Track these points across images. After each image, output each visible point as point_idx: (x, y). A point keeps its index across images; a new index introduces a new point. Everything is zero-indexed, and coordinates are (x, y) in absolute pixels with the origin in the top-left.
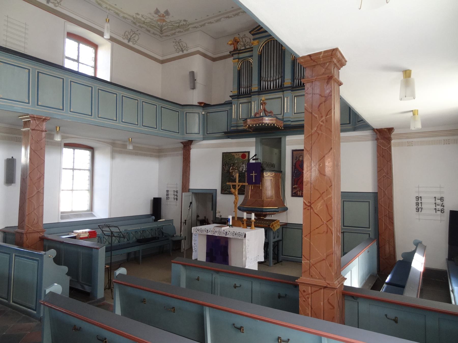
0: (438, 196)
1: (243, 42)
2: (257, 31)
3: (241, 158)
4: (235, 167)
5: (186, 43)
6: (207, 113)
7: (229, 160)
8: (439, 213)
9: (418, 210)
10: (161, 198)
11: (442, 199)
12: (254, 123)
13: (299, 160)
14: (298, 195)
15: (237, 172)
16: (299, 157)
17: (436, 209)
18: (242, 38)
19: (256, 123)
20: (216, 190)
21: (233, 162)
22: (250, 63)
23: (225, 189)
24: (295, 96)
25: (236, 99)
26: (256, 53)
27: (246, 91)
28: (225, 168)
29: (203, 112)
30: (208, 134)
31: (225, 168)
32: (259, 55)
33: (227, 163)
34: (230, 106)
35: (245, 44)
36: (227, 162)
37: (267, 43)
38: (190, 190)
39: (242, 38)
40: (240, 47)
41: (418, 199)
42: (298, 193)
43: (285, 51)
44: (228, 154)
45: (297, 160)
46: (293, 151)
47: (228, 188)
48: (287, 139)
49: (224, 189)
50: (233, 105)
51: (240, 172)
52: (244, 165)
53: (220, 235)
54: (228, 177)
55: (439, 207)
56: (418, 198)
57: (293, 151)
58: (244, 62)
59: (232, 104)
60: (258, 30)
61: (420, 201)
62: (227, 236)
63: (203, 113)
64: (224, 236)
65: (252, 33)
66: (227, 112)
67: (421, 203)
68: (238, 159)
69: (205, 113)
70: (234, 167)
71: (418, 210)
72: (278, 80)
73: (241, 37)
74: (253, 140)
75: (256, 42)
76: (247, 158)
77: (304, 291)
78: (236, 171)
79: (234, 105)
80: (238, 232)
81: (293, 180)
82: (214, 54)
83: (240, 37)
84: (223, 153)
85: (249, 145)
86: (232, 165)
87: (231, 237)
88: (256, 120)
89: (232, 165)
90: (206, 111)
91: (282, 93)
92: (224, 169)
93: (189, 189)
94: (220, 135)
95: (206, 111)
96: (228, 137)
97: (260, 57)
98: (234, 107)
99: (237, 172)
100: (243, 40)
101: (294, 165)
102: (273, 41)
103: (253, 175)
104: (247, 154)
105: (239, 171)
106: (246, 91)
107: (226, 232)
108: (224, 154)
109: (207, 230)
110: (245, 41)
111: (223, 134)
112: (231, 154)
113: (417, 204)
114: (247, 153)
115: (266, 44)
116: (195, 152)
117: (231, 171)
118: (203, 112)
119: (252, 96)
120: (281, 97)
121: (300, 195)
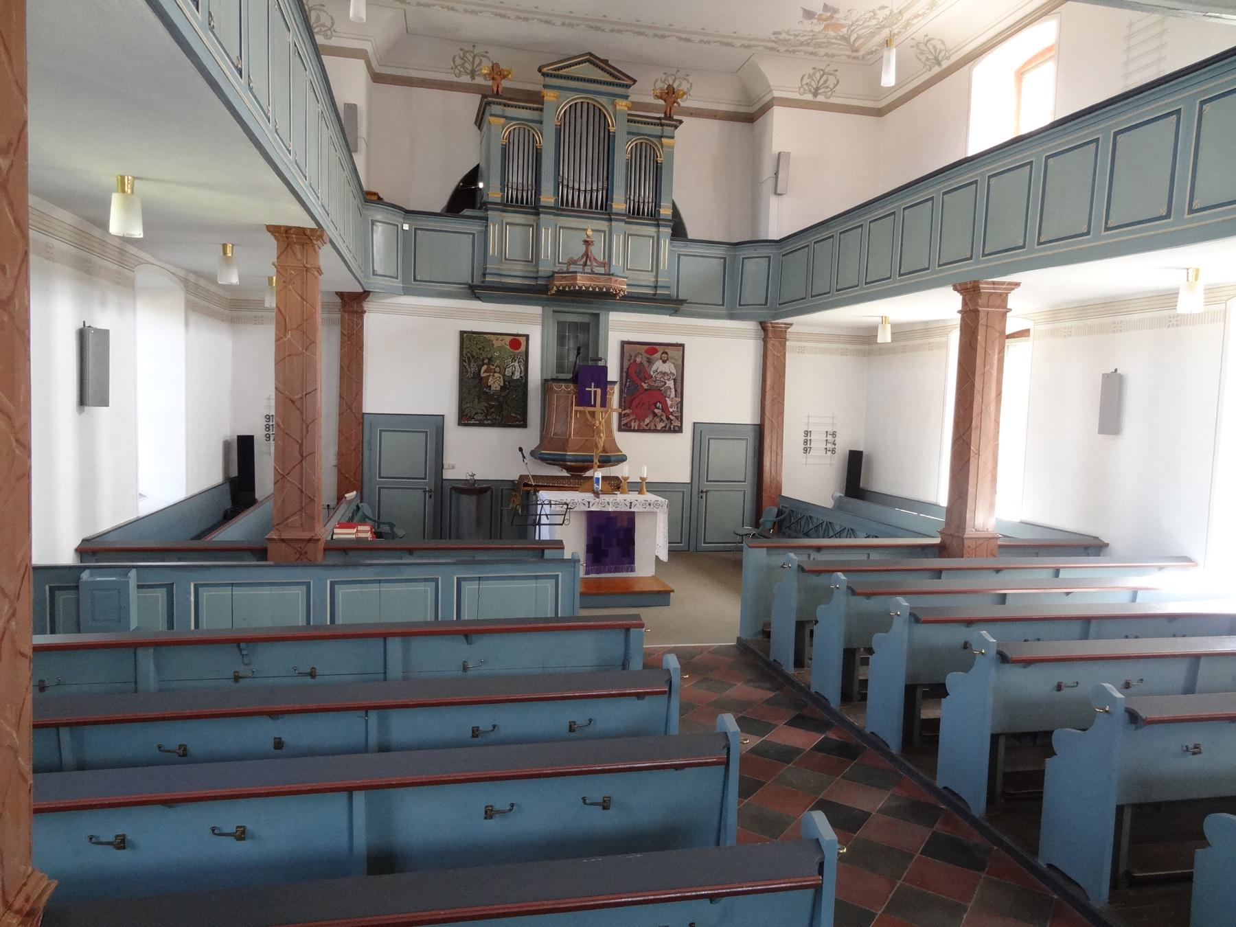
0: (830, 430)
1: (473, 64)
3: (508, 347)
4: (493, 365)
5: (332, 19)
6: (416, 229)
7: (480, 349)
8: (829, 453)
9: (806, 450)
10: (253, 436)
11: (834, 434)
13: (635, 361)
14: (632, 428)
15: (500, 377)
16: (636, 356)
17: (826, 449)
20: (443, 416)
21: (489, 356)
22: (531, 136)
23: (469, 414)
24: (629, 235)
26: (551, 120)
27: (520, 197)
28: (470, 367)
29: (404, 223)
30: (417, 281)
31: (470, 367)
32: (556, 125)
33: (473, 357)
34: (480, 224)
36: (474, 354)
37: (574, 106)
38: (365, 416)
40: (460, 71)
41: (807, 434)
42: (633, 424)
44: (474, 335)
45: (632, 361)
46: (624, 344)
47: (476, 413)
48: (610, 316)
49: (467, 415)
51: (506, 378)
52: (516, 364)
53: (618, 509)
54: (477, 389)
55: (830, 446)
56: (807, 433)
57: (624, 344)
60: (558, 69)
61: (809, 438)
62: (632, 510)
63: (406, 227)
64: (627, 509)
65: (545, 70)
66: (471, 236)
67: (810, 440)
68: (500, 349)
70: (492, 367)
71: (806, 451)
72: (595, 193)
73: (475, 53)
74: (537, 310)
75: (552, 95)
76: (523, 348)
77: (969, 547)
78: (496, 375)
79: (494, 225)
80: (653, 500)
81: (623, 400)
84: (462, 333)
85: (526, 319)
86: (486, 361)
87: (641, 510)
89: (486, 361)
92: (465, 370)
93: (364, 414)
94: (452, 289)
96: (478, 298)
97: (558, 131)
98: (494, 229)
99: (500, 377)
100: (473, 61)
101: (625, 370)
102: (586, 104)
103: (591, 391)
104: (523, 340)
105: (504, 375)
106: (520, 197)
107: (631, 503)
108: (465, 335)
109: (589, 503)
111: (463, 288)
112: (485, 336)
113: (806, 442)
114: (525, 338)
115: (570, 106)
116: (375, 322)
117: (483, 375)
119: (542, 216)
120: (604, 232)
121: (636, 428)
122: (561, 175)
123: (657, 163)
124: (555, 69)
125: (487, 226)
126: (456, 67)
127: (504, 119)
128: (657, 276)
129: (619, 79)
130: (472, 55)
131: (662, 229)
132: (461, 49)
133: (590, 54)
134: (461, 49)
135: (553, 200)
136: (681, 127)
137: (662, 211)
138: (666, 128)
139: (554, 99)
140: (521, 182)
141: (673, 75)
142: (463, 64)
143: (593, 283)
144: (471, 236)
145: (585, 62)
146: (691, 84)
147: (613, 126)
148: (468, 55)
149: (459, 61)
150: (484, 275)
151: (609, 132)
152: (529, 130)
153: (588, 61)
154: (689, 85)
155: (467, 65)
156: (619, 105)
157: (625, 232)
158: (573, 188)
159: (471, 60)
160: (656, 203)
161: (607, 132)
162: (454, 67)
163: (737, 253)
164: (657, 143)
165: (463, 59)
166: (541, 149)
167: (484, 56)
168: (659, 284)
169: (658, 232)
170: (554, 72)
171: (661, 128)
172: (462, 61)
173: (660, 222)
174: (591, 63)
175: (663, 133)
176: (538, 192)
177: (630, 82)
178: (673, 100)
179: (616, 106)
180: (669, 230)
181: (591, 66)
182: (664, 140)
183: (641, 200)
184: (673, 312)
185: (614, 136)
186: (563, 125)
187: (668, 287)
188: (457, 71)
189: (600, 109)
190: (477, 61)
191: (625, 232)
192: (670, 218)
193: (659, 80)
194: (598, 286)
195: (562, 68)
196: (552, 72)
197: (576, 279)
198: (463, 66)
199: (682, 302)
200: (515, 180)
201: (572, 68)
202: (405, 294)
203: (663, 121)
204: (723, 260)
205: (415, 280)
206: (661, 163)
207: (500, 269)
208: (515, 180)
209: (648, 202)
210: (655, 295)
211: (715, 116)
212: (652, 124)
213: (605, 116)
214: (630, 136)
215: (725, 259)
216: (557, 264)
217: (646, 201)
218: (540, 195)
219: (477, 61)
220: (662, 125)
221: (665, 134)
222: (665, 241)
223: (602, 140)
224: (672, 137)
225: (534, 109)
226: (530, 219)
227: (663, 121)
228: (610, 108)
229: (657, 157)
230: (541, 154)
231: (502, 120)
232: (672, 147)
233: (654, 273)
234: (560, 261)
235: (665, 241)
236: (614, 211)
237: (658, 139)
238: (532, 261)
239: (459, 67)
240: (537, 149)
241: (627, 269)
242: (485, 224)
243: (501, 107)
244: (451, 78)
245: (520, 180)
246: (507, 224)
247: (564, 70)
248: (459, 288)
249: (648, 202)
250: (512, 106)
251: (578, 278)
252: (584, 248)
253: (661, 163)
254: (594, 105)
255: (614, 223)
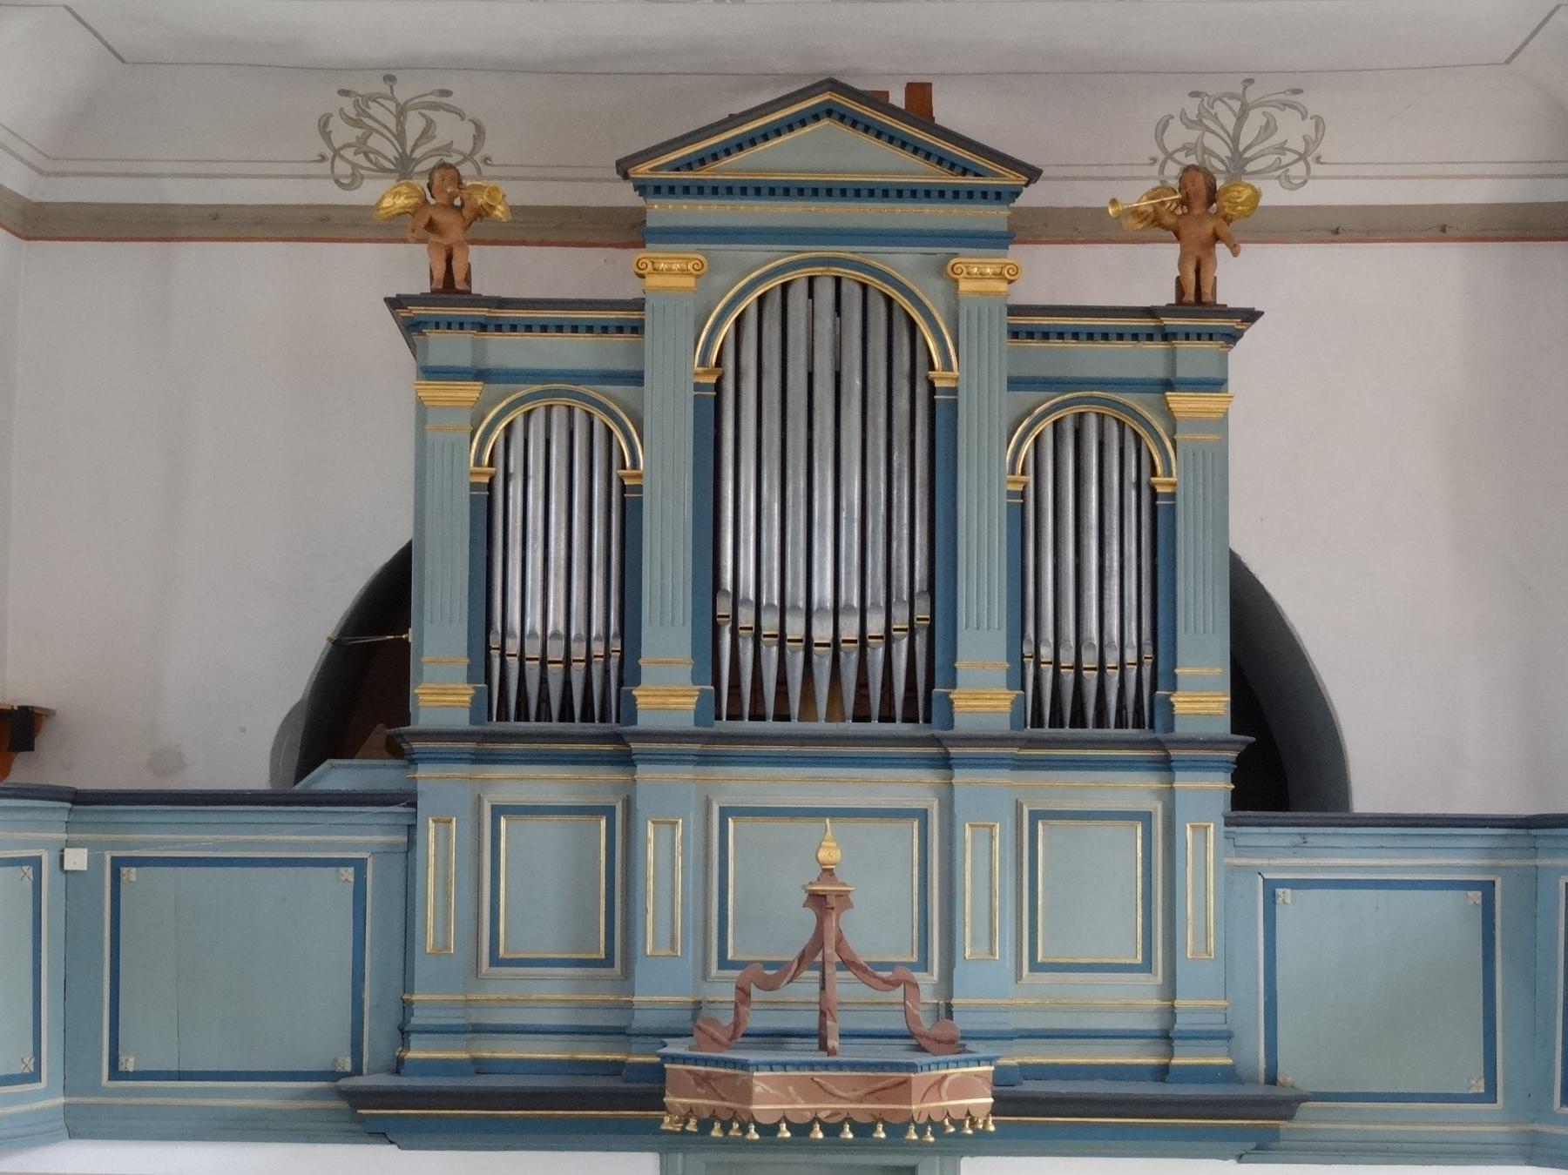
1: (400, 136)
2: (689, 167)
6: (118, 864)
12: (817, 1111)
18: (401, 113)
19: (835, 1113)
24: (1035, 816)
25: (463, 770)
30: (127, 1076)
32: (698, 386)
34: (387, 820)
35: (418, 154)
39: (401, 113)
40: (354, 166)
43: (956, 401)
50: (431, 824)
58: (528, 415)
59: (414, 805)
60: (701, 160)
63: (77, 859)
65: (642, 171)
66: (348, 873)
69: (94, 861)
82: (41, 173)
83: (393, 99)
88: (831, 1087)
90: (113, 845)
91: (928, 776)
95: (113, 845)
100: (400, 124)
110: (427, 133)
115: (761, 300)
118: (69, 853)
120: (923, 815)
122: (728, 586)
123: (1154, 495)
124: (687, 165)
125: (411, 829)
126: (337, 153)
127: (478, 386)
128: (1170, 989)
129: (965, 172)
130: (392, 106)
131: (1185, 782)
132: (344, 93)
133: (833, 85)
134: (344, 93)
135: (690, 703)
136: (1253, 333)
137: (1182, 703)
138: (1182, 346)
139: (690, 282)
140: (561, 629)
141: (1232, 96)
142: (363, 140)
143: (825, 1108)
144: (348, 873)
145: (817, 118)
146: (1319, 123)
147: (947, 366)
148: (374, 109)
149: (343, 133)
150: (404, 1033)
151: (932, 390)
152: (590, 416)
153: (829, 113)
154: (1311, 124)
155: (375, 142)
156: (970, 276)
157: (1019, 807)
158: (782, 638)
159: (391, 122)
160: (1155, 665)
161: (921, 390)
162: (329, 154)
163: (1539, 862)
164: (1139, 408)
165: (355, 123)
166: (639, 488)
167: (436, 107)
168: (1182, 1024)
169: (1169, 798)
170: (674, 175)
171: (1158, 346)
172: (359, 132)
173: (1173, 764)
174: (842, 118)
175: (1174, 371)
176: (629, 672)
177: (1011, 179)
178: (1209, 227)
179: (957, 281)
180: (1219, 785)
181: (845, 131)
182: (1180, 402)
183: (1090, 659)
184: (1254, 1145)
185: (954, 406)
186: (729, 385)
187: (1227, 1036)
188: (342, 168)
189: (889, 301)
190: (414, 126)
191: (1019, 807)
192: (1223, 727)
193: (1177, 118)
194: (849, 1119)
195: (701, 160)
196: (674, 175)
197: (746, 1094)
198: (361, 147)
199: (1285, 1106)
200: (534, 620)
201: (761, 148)
202: (73, 1135)
203: (1168, 321)
204: (1476, 896)
205: (116, 1073)
206: (1172, 496)
207: (468, 1003)
208: (534, 620)
209: (1122, 665)
210: (1162, 1073)
211: (1443, 230)
212: (1120, 337)
213: (913, 326)
214: (1028, 397)
215: (1487, 889)
216: (714, 970)
217: (1112, 659)
218: (637, 683)
219: (414, 126)
220: (1167, 335)
221: (1183, 372)
222: (1201, 831)
223: (901, 423)
224: (1217, 384)
225: (605, 330)
226: (598, 782)
227: (1168, 321)
228: (932, 294)
229: (1154, 473)
230: (640, 501)
231: (471, 391)
232: (1221, 424)
233: (1159, 977)
234: (730, 955)
235: (1201, 831)
236: (962, 725)
237: (1150, 397)
238: (608, 962)
239: (348, 153)
240: (623, 488)
241: (1035, 967)
242: (406, 821)
243: (466, 338)
244: (325, 193)
245: (556, 620)
246: (497, 811)
247: (726, 162)
248: (311, 1094)
249: (1122, 665)
250: (514, 328)
251: (759, 1088)
252: (810, 916)
253: (1172, 496)
254: (864, 287)
255: (961, 777)
